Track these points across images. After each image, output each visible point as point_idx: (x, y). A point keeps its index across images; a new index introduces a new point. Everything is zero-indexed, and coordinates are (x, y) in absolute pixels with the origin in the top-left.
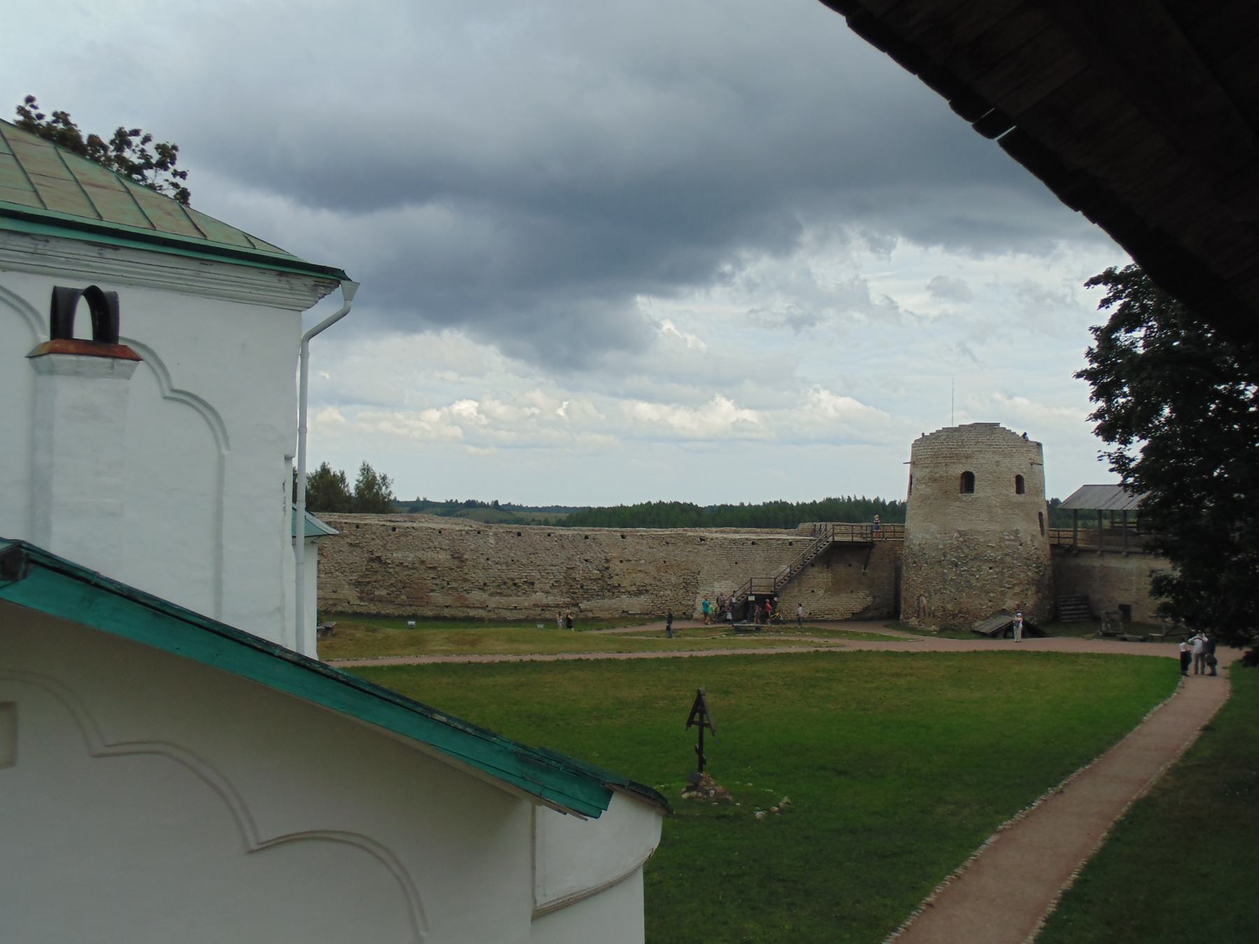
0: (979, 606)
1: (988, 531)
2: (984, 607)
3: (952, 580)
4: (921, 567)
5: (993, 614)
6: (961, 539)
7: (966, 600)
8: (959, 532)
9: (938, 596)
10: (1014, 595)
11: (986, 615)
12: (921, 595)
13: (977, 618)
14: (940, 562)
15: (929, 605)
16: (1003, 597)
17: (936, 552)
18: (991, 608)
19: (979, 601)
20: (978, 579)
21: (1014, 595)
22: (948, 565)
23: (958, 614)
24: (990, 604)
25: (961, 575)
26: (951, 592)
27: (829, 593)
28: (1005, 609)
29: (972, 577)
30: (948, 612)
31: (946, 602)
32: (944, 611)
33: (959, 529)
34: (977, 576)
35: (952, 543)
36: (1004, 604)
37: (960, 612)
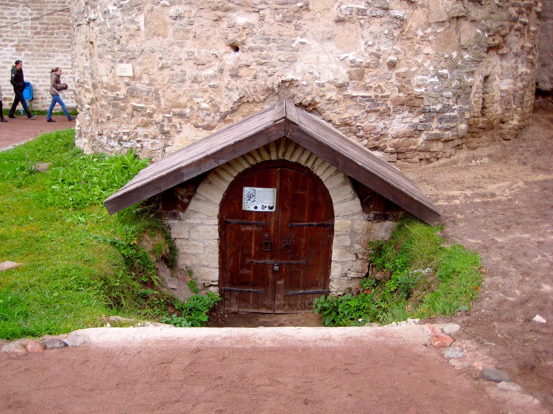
0: (190, 70)
2: (210, 72)
5: (241, 102)
7: (148, 45)
10: (340, 21)
11: (215, 106)
13: (181, 115)
16: (288, 30)
18: (235, 76)
19: (190, 45)
21: (340, 21)
23: (125, 100)
24: (231, 58)
27: (27, 52)
28: (291, 82)
30: (102, 91)
32: (95, 86)
36: (292, 61)
37: (132, 93)
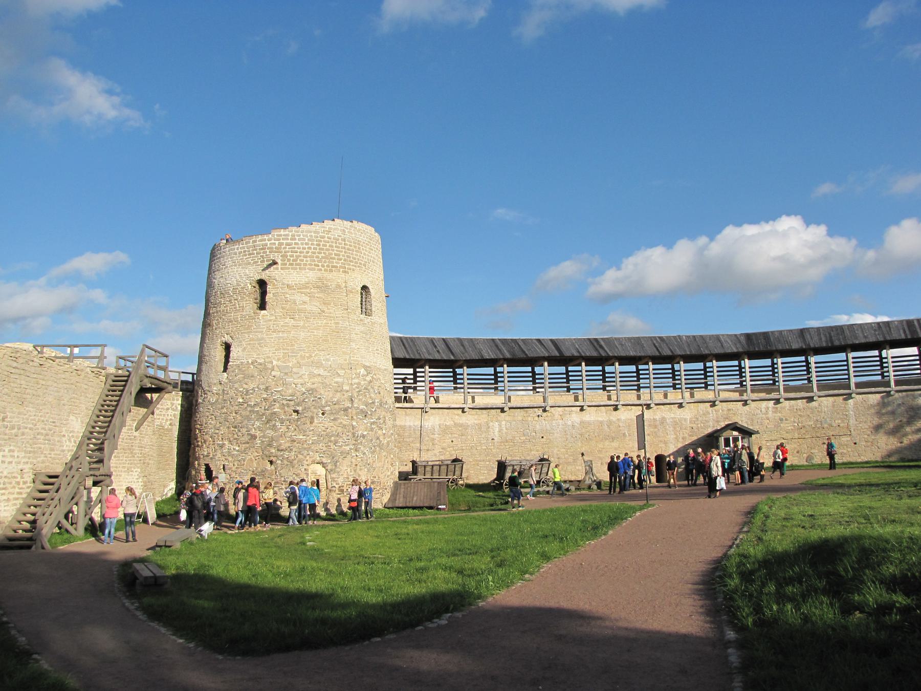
1: (385, 370)
3: (363, 436)
4: (312, 418)
6: (368, 378)
8: (365, 367)
9: (347, 462)
12: (313, 462)
14: (346, 410)
15: (334, 476)
17: (338, 395)
20: (384, 434)
22: (357, 414)
25: (372, 429)
26: (364, 454)
29: (380, 432)
31: (358, 467)
33: (367, 364)
34: (384, 432)
35: (359, 384)
